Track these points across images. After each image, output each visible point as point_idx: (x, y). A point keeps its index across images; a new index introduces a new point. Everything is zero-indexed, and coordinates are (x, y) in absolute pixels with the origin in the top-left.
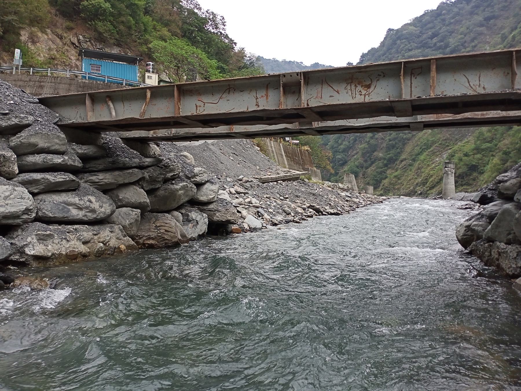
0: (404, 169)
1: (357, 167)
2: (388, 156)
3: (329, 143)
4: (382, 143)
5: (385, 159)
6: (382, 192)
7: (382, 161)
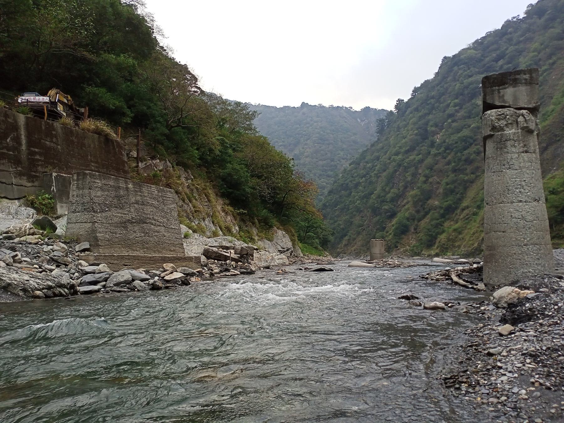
0: (467, 219)
1: (408, 219)
2: (445, 203)
3: (375, 192)
4: (437, 189)
5: (441, 208)
6: (437, 251)
7: (438, 210)
